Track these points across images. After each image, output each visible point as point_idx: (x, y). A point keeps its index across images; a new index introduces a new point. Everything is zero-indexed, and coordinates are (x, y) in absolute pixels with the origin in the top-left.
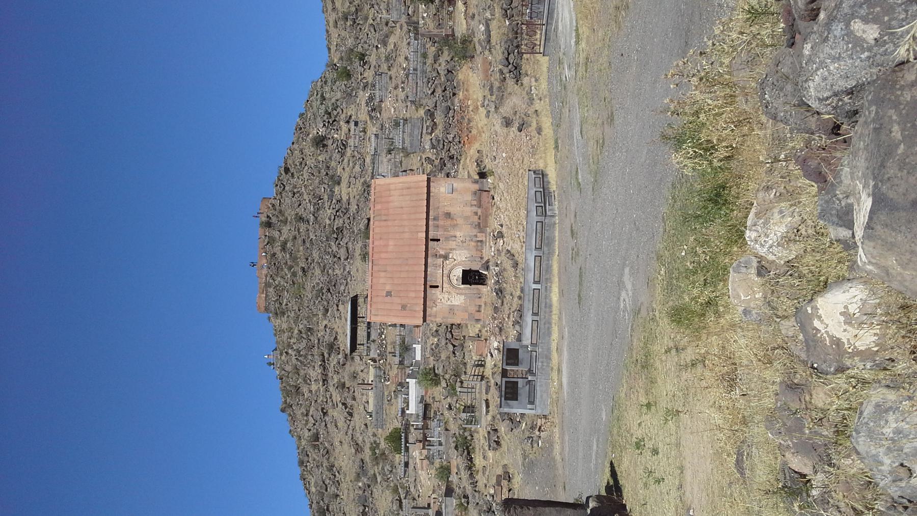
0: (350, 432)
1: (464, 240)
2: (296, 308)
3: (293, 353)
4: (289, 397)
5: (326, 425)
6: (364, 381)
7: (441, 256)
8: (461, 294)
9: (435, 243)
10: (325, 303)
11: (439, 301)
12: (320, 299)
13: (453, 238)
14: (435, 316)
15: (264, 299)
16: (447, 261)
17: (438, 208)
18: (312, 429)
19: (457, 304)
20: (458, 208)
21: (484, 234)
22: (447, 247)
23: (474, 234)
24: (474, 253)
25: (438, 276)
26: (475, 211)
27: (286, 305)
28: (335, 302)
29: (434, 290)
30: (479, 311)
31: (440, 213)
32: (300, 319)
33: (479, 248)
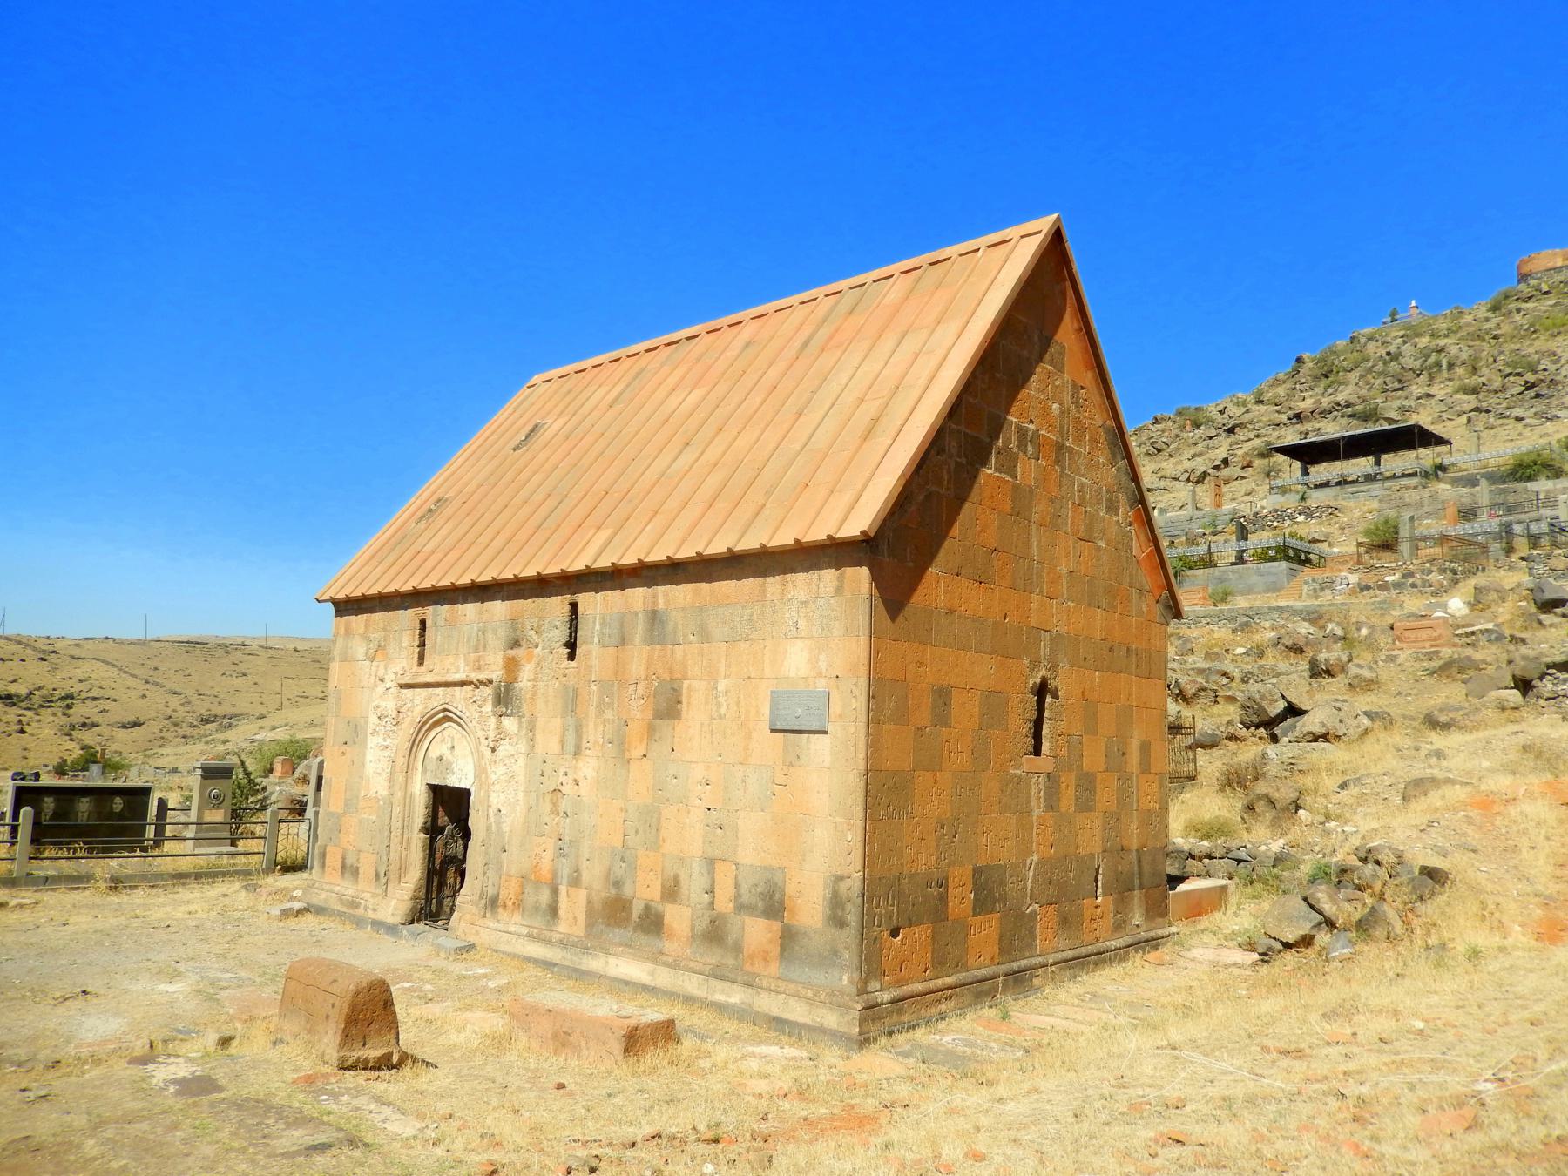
0: (1162, 484)
1: (564, 805)
2: (1506, 328)
3: (1392, 349)
4: (1317, 363)
5: (1211, 438)
6: (1249, 494)
7: (512, 666)
8: (391, 780)
9: (562, 634)
10: (1497, 384)
11: (381, 673)
12: (1508, 370)
13: (571, 738)
14: (344, 659)
15: (1551, 265)
16: (488, 708)
17: (704, 636)
18: (1225, 416)
19: (370, 756)
20: (699, 773)
21: (579, 930)
22: (540, 703)
23: (584, 865)
24: (515, 862)
25: (451, 659)
26: (684, 890)
27: (1518, 310)
28: (1484, 404)
29: (409, 640)
30: (344, 867)
31: (679, 651)
32: (1471, 343)
33: (530, 899)
